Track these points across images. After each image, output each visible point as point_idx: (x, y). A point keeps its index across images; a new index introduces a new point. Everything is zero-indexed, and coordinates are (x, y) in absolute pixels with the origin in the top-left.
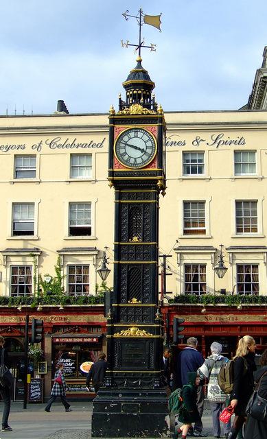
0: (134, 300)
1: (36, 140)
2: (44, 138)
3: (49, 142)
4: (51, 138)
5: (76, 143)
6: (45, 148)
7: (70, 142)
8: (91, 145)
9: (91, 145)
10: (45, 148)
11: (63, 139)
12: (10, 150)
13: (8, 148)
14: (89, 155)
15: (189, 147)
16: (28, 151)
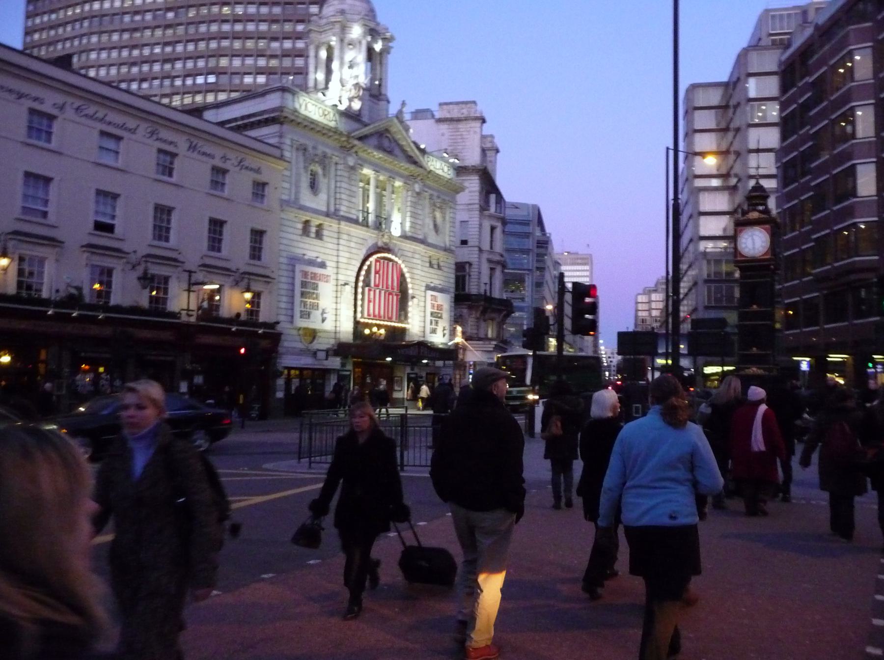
0: (754, 349)
1: (59, 99)
2: (70, 100)
3: (75, 106)
4: (78, 103)
5: (108, 119)
6: (70, 113)
7: (100, 115)
8: (122, 127)
9: (122, 127)
10: (70, 113)
11: (92, 110)
12: (23, 100)
13: (21, 96)
14: (119, 139)
15: (218, 162)
16: (46, 108)
